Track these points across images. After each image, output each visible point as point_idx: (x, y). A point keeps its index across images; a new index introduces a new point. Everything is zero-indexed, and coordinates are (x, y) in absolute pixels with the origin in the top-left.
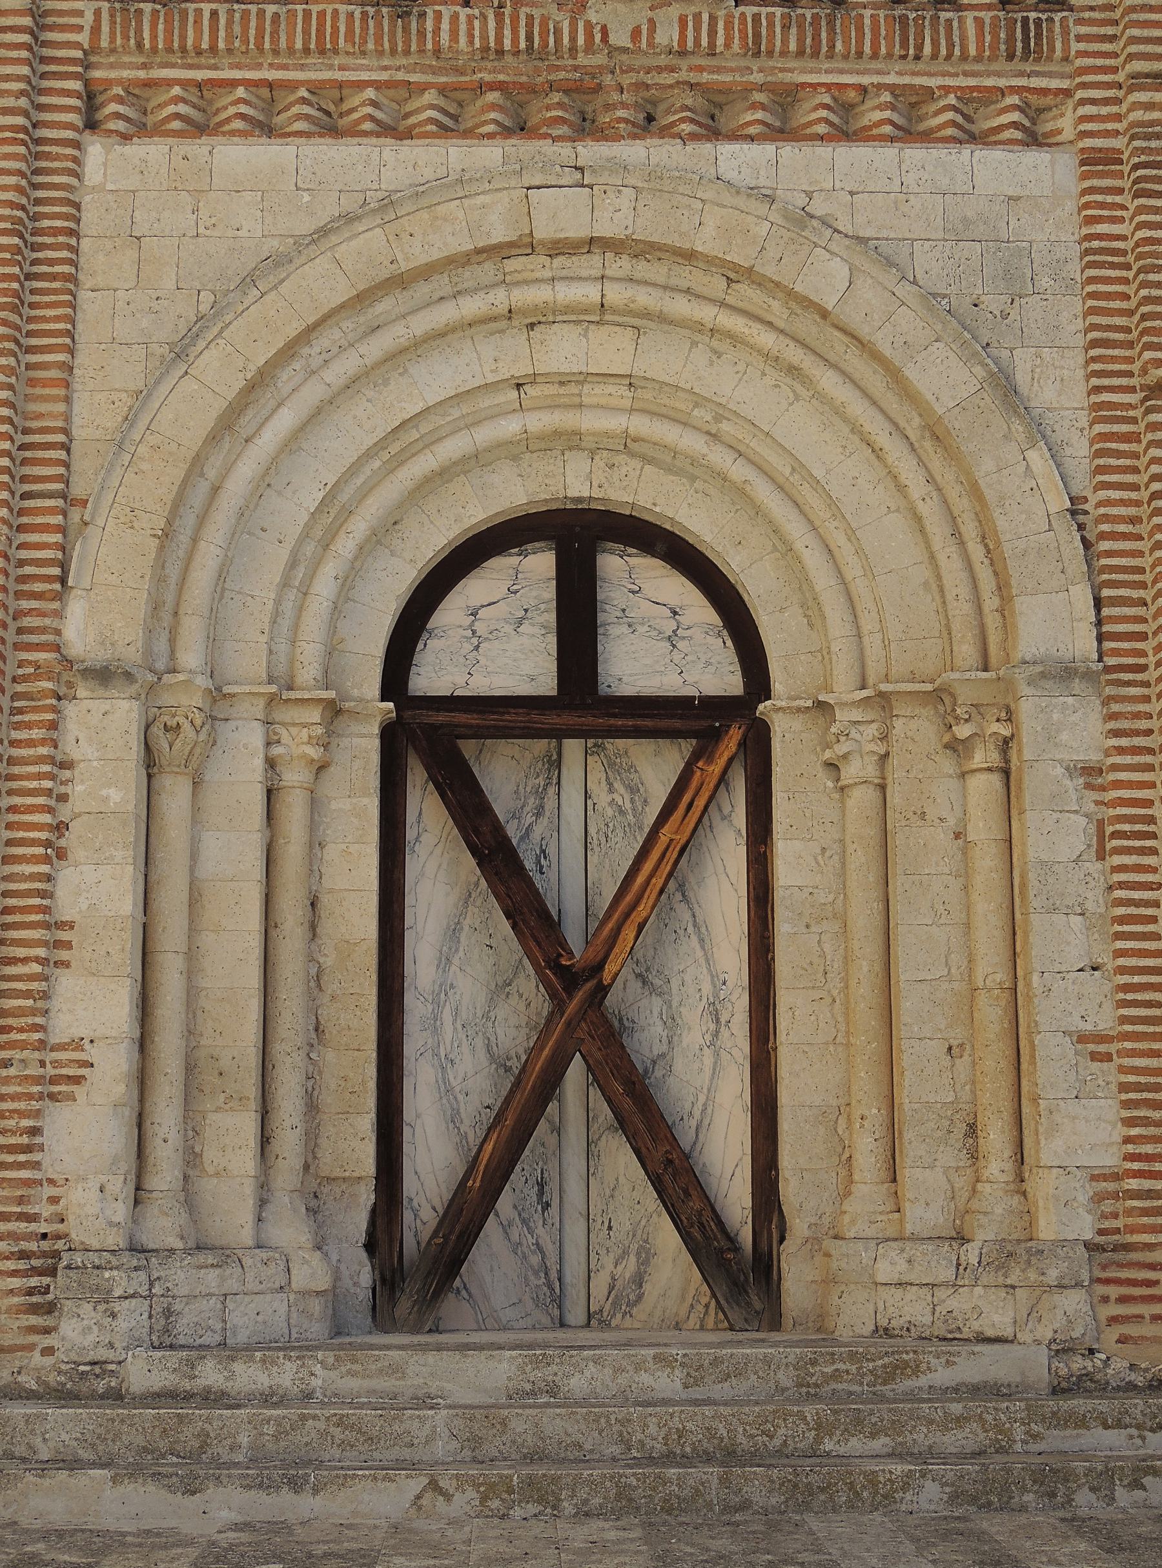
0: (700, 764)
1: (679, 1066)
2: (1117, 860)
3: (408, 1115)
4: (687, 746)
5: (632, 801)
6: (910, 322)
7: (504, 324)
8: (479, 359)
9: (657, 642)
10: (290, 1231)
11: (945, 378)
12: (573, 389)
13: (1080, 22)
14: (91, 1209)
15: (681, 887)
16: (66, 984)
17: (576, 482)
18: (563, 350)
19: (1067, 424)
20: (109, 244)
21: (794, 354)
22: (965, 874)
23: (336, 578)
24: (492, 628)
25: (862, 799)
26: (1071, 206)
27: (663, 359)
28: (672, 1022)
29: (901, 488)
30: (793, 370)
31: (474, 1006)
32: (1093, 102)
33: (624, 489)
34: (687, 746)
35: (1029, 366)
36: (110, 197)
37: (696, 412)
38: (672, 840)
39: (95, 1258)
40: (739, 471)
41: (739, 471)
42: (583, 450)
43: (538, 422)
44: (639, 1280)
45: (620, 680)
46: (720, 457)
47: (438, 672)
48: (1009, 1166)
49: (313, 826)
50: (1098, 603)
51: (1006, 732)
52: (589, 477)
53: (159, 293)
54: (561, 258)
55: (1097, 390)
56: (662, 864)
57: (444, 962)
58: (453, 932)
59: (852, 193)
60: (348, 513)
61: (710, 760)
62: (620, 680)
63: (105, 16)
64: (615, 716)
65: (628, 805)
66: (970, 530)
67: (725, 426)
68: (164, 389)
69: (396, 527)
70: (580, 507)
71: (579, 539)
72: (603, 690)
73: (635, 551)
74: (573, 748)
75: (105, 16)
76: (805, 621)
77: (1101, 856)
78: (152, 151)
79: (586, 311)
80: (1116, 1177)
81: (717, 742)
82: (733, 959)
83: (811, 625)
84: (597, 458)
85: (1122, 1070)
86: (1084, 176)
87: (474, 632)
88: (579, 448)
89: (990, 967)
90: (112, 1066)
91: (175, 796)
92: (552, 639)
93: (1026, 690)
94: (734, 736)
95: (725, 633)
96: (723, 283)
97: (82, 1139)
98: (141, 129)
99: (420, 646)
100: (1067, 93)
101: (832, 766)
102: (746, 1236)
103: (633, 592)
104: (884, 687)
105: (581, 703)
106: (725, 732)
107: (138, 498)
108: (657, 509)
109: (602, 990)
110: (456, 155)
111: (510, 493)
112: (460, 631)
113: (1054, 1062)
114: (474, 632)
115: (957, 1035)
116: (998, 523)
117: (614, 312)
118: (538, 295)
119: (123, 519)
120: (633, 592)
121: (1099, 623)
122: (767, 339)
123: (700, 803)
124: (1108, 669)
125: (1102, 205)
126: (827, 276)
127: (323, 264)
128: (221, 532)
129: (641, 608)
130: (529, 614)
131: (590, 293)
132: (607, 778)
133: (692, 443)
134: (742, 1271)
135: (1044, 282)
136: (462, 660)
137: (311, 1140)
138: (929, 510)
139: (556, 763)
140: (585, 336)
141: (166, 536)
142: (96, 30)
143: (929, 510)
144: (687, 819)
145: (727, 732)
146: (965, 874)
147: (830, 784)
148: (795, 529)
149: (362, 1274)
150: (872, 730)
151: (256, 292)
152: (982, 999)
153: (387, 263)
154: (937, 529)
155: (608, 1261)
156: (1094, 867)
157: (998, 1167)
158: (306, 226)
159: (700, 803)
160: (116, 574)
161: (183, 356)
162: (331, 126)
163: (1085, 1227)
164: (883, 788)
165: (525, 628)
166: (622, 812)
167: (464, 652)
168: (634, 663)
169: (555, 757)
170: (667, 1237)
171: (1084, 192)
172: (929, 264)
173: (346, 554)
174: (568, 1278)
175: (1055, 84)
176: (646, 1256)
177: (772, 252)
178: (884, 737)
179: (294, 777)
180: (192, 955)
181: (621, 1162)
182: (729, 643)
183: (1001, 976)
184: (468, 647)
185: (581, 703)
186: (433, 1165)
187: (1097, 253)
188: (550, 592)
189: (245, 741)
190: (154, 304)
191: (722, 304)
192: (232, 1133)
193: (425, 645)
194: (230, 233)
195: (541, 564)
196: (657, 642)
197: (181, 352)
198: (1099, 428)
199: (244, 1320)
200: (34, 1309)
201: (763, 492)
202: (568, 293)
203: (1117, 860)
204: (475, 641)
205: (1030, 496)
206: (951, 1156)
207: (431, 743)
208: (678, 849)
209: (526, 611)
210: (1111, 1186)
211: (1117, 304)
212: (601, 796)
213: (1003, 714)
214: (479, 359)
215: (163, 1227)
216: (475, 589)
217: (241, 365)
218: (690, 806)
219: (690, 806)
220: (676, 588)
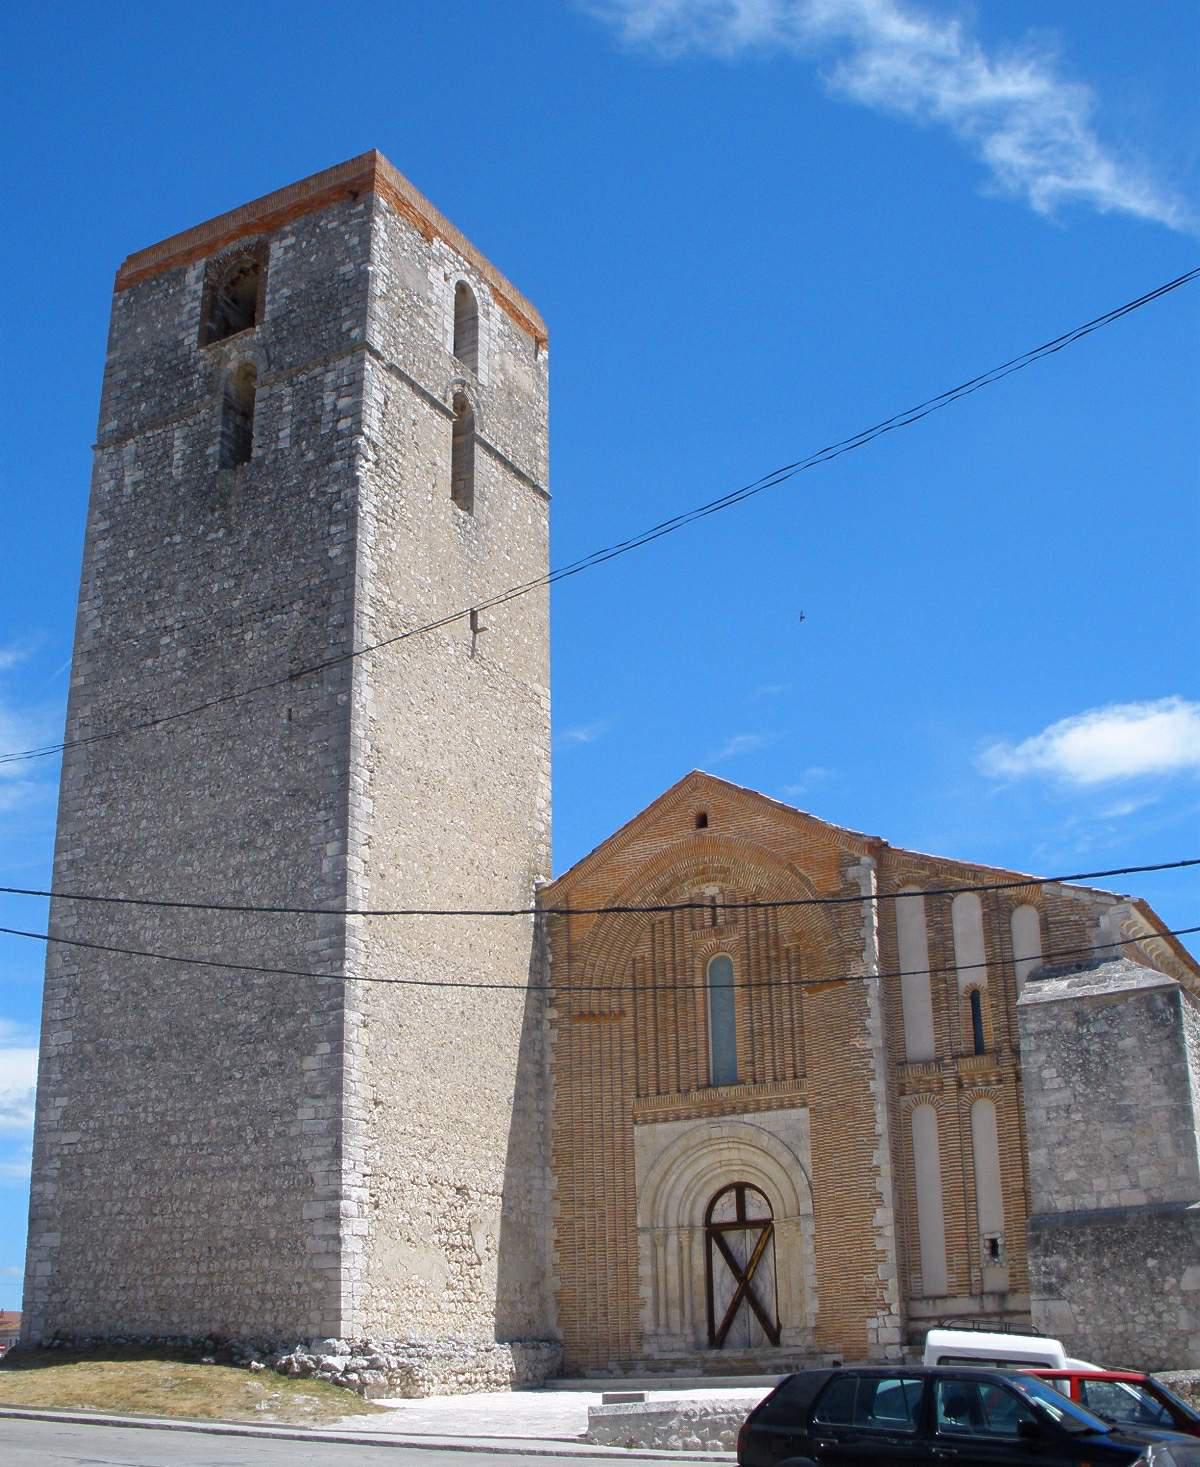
6: (780, 1148)
10: (688, 1331)
11: (786, 1159)
14: (648, 1327)
16: (642, 1288)
17: (736, 1178)
18: (726, 1155)
31: (726, 1285)
46: (757, 1173)
47: (716, 1219)
49: (690, 1253)
56: (759, 1255)
57: (722, 1277)
58: (723, 1271)
60: (692, 1189)
71: (740, 1188)
74: (748, 1231)
78: (646, 1127)
90: (650, 1303)
91: (660, 1250)
97: (646, 1314)
98: (645, 1122)
105: (742, 1222)
110: (698, 1122)
113: (808, 1292)
126: (765, 1140)
134: (774, 1335)
137: (693, 1314)
141: (654, 1202)
149: (704, 1337)
162: (677, 1118)
163: (813, 1325)
168: (752, 1213)
172: (782, 1135)
179: (685, 1244)
180: (666, 1280)
186: (720, 1316)
187: (813, 1130)
189: (673, 1241)
192: (675, 1314)
195: (734, 1193)
197: (652, 1167)
199: (676, 1346)
202: (722, 1146)
205: (802, 1184)
207: (714, 1233)
215: (661, 1331)
216: (723, 1200)
220: (760, 1197)
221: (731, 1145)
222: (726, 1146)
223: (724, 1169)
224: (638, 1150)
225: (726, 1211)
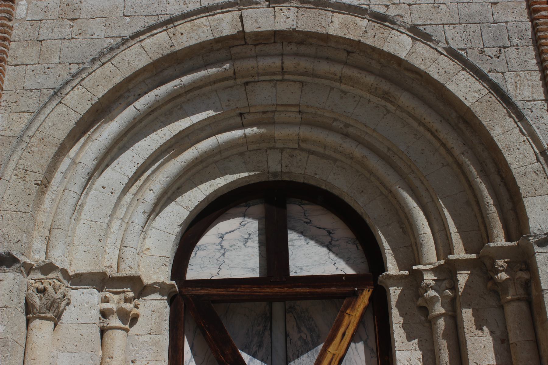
0: (348, 311)
5: (311, 337)
7: (231, 82)
8: (220, 100)
17: (275, 165)
19: (538, 107)
20: (26, 44)
21: (385, 86)
23: (144, 213)
24: (231, 244)
29: (449, 151)
33: (299, 167)
35: (513, 80)
36: (28, 23)
37: (335, 124)
38: (334, 355)
40: (358, 152)
42: (277, 149)
45: (301, 269)
46: (349, 146)
51: (525, 276)
52: (280, 162)
53: (50, 66)
54: (260, 46)
59: (409, 5)
61: (353, 309)
62: (301, 269)
64: (299, 287)
65: (309, 339)
67: (351, 130)
68: (47, 111)
69: (179, 191)
70: (277, 179)
72: (292, 274)
73: (307, 202)
76: (401, 230)
79: (274, 74)
81: (356, 300)
83: (404, 232)
84: (284, 153)
87: (222, 246)
88: (274, 148)
93: (537, 249)
94: (365, 297)
95: (357, 242)
96: (345, 54)
99: (193, 255)
103: (307, 223)
107: (29, 165)
108: (317, 176)
112: (215, 246)
114: (222, 246)
116: (508, 160)
117: (290, 73)
119: (20, 176)
120: (307, 223)
122: (370, 79)
127: (136, 48)
128: (77, 185)
130: (251, 237)
131: (275, 63)
132: (297, 325)
135: (515, 41)
136: (215, 261)
139: (268, 318)
140: (275, 86)
144: (342, 342)
145: (362, 293)
147: (423, 318)
151: (99, 63)
153: (168, 47)
158: (127, 33)
160: (13, 205)
161: (59, 94)
165: (249, 244)
167: (216, 257)
169: (268, 315)
173: (149, 201)
177: (370, 33)
182: (360, 247)
184: (219, 254)
190: (47, 70)
191: (345, 64)
193: (196, 254)
194: (88, 37)
204: (222, 251)
208: (338, 360)
209: (250, 234)
212: (294, 335)
213: (523, 267)
214: (220, 100)
216: (222, 226)
217: (90, 98)
218: (344, 334)
219: (344, 334)
222: (275, 63)
225: (232, 252)
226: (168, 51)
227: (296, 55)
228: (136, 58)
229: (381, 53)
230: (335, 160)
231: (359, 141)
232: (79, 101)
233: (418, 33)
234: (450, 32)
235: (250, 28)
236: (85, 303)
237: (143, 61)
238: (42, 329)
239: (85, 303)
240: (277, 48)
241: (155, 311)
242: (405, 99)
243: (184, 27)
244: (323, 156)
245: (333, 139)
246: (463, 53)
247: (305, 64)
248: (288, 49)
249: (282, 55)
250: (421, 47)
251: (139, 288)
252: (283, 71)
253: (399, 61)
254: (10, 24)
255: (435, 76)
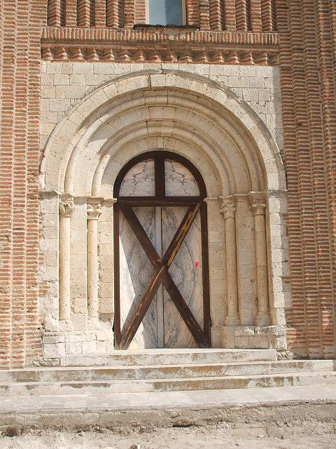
1: (185, 285)
2: (291, 236)
3: (121, 298)
4: (186, 209)
9: (179, 183)
12: (160, 122)
13: (281, 36)
15: (185, 242)
17: (160, 145)
18: (157, 114)
21: (214, 115)
22: (254, 239)
25: (229, 222)
26: (279, 80)
27: (181, 117)
28: (183, 274)
30: (213, 119)
32: (284, 55)
34: (186, 209)
39: (50, 333)
40: (199, 142)
41: (199, 142)
43: (151, 130)
44: (176, 336)
46: (195, 139)
47: (126, 191)
48: (266, 308)
50: (286, 176)
55: (285, 125)
61: (193, 212)
63: (45, 31)
66: (256, 157)
67: (196, 132)
71: (160, 158)
72: (166, 195)
74: (158, 209)
75: (45, 31)
77: (287, 235)
80: (292, 310)
82: (198, 258)
83: (217, 179)
85: (293, 285)
86: (282, 74)
89: (261, 262)
92: (154, 182)
100: (278, 53)
101: (222, 214)
102: (202, 326)
104: (235, 195)
106: (196, 206)
109: (167, 268)
111: (144, 147)
115: (253, 278)
118: (152, 100)
121: (287, 180)
122: (207, 111)
123: (190, 222)
124: (288, 191)
125: (287, 80)
126: (221, 97)
127: (101, 92)
129: (175, 175)
131: (165, 100)
133: (187, 135)
138: (246, 153)
142: (43, 33)
143: (246, 153)
146: (254, 239)
148: (213, 156)
150: (232, 205)
152: (259, 269)
154: (248, 158)
155: (169, 332)
156: (285, 238)
157: (263, 308)
158: (97, 83)
159: (190, 222)
164: (234, 219)
166: (171, 224)
170: (183, 326)
171: (282, 77)
174: (159, 336)
175: (275, 50)
176: (178, 331)
178: (235, 207)
181: (172, 308)
183: (264, 264)
184: (133, 185)
185: (160, 199)
188: (153, 171)
191: (196, 102)
195: (150, 164)
196: (179, 183)
198: (286, 134)
200: (37, 346)
201: (206, 148)
202: (159, 100)
203: (291, 236)
206: (252, 306)
207: (125, 208)
210: (289, 312)
211: (290, 104)
212: (165, 220)
216: (136, 170)
220: (182, 170)
221: (171, 100)
222: (165, 100)
223: (151, 130)
224: (44, 91)
225: (141, 184)
226: (116, 94)
227: (174, 96)
228: (101, 97)
229: (213, 100)
230: (188, 144)
231: (200, 137)
232: (77, 118)
233: (230, 93)
234: (245, 92)
235: (154, 84)
236: (81, 211)
237: (105, 100)
238: (67, 222)
239: (81, 211)
240: (165, 93)
241: (107, 213)
242: (222, 122)
243: (123, 82)
244: (182, 142)
245: (187, 135)
246: (249, 104)
247: (178, 101)
248: (170, 93)
249: (167, 96)
250: (233, 101)
251: (102, 201)
252: (167, 103)
253: (221, 105)
254: (39, 75)
255: (236, 114)
